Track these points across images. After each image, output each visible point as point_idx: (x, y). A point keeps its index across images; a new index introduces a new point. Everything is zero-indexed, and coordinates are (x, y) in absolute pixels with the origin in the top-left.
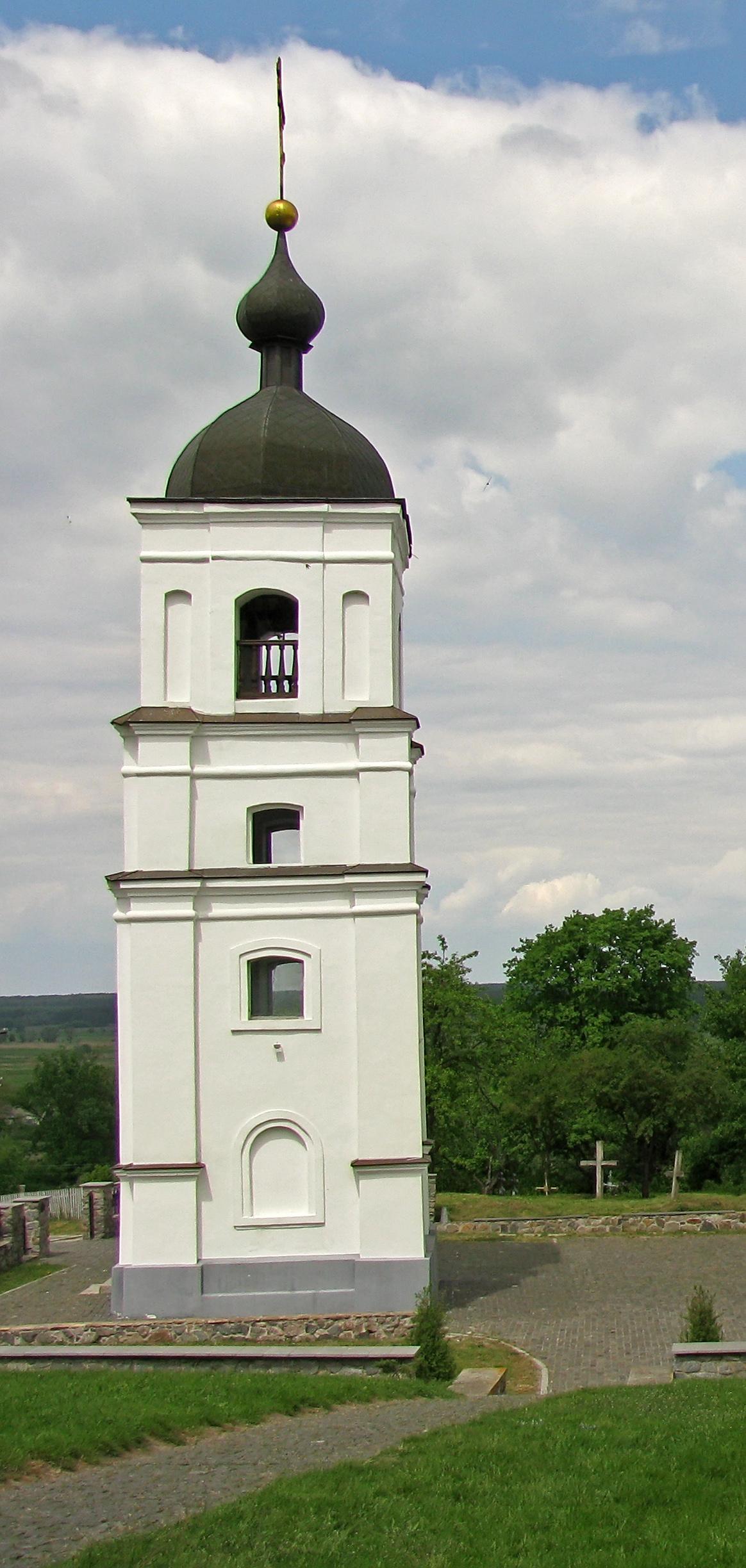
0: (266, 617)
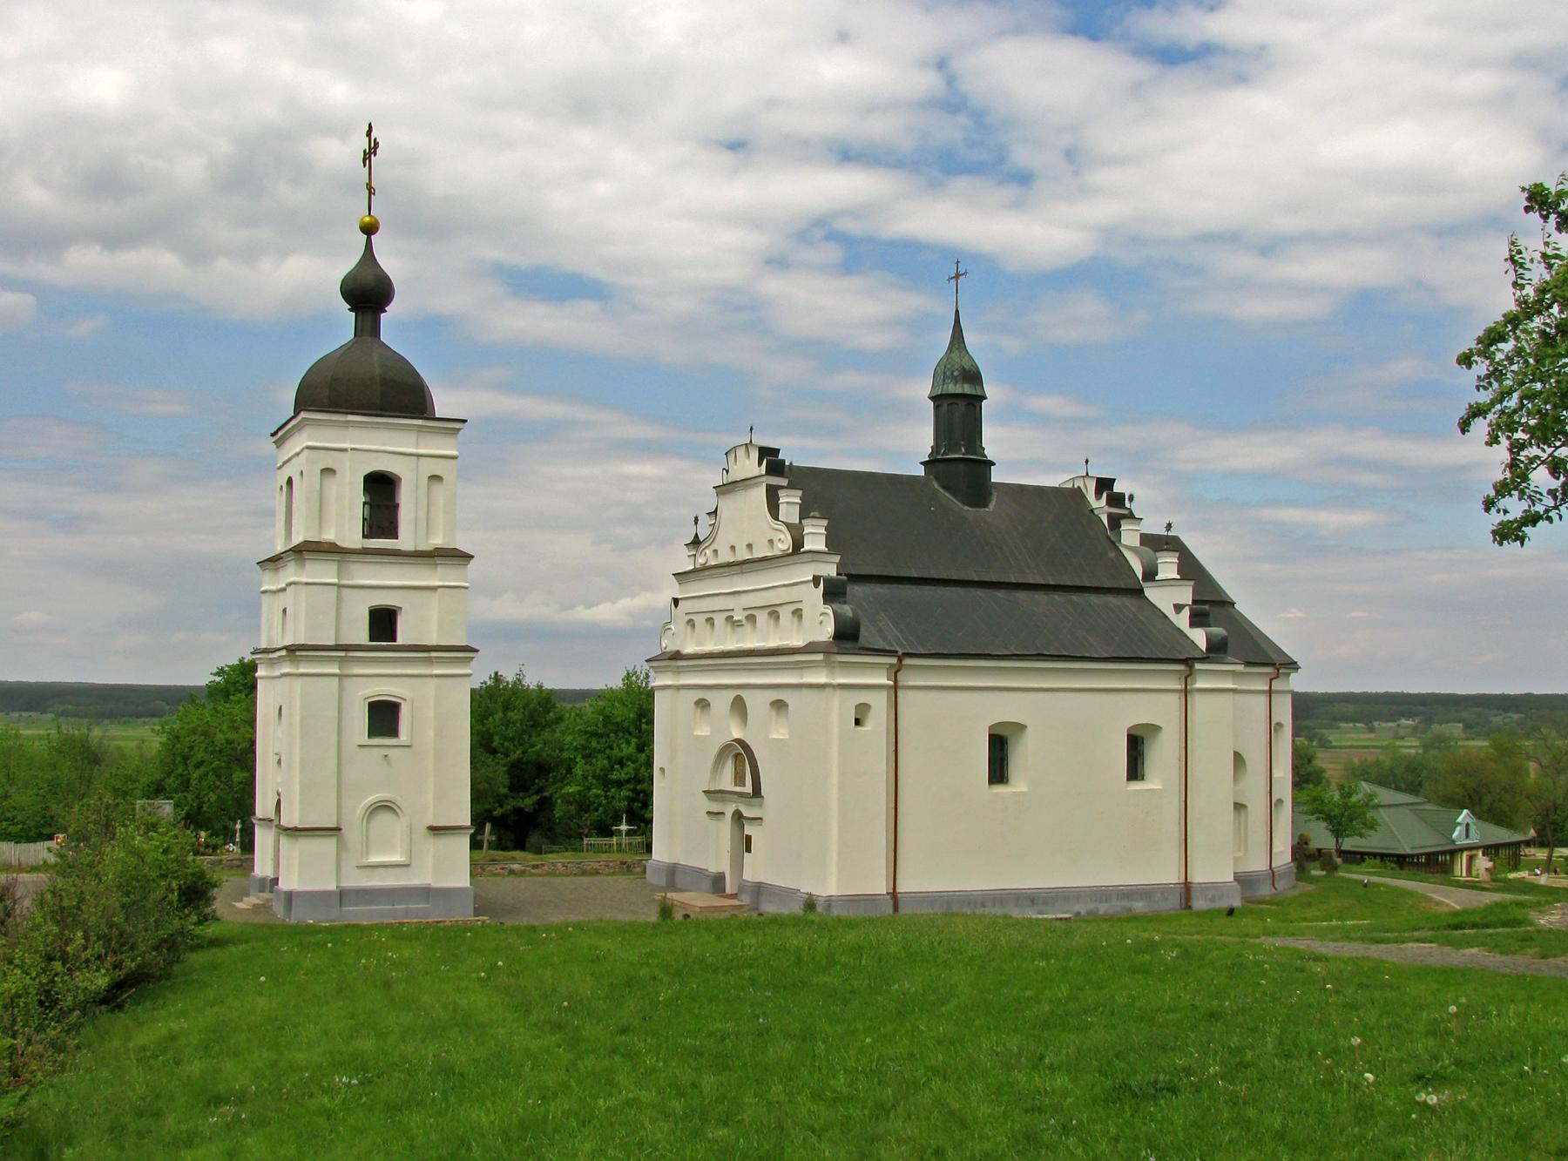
0: (381, 487)
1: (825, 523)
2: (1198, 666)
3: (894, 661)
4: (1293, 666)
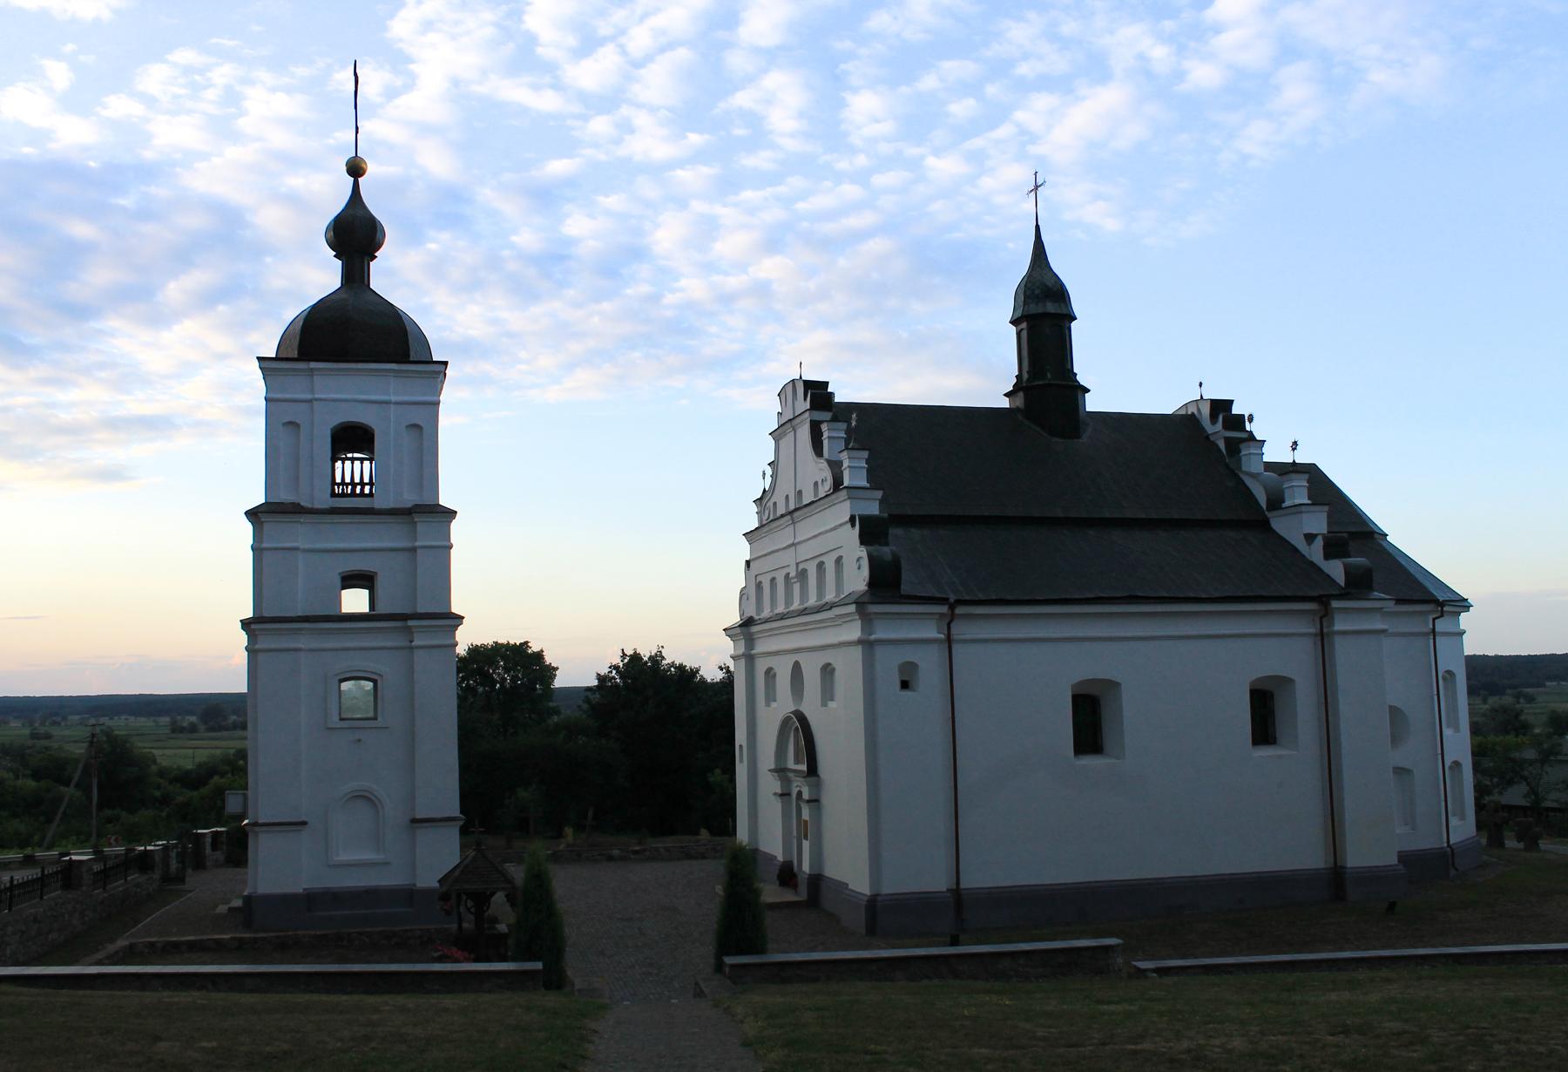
1: (865, 454)
2: (1335, 604)
3: (944, 609)
4: (1462, 604)
